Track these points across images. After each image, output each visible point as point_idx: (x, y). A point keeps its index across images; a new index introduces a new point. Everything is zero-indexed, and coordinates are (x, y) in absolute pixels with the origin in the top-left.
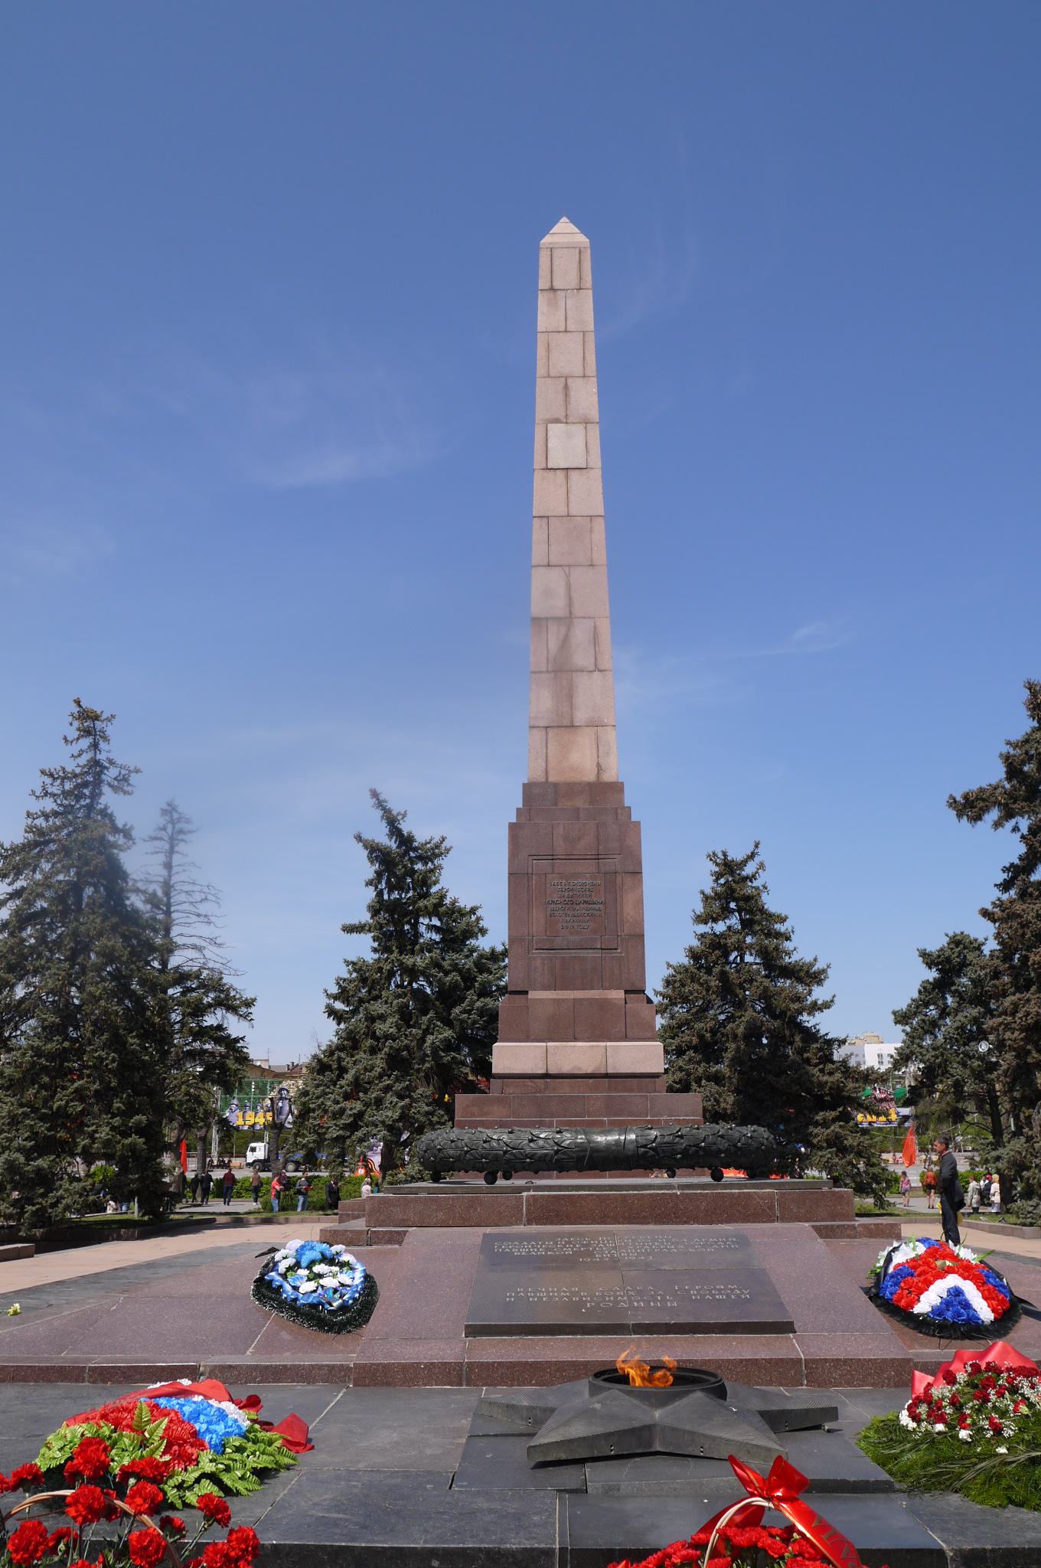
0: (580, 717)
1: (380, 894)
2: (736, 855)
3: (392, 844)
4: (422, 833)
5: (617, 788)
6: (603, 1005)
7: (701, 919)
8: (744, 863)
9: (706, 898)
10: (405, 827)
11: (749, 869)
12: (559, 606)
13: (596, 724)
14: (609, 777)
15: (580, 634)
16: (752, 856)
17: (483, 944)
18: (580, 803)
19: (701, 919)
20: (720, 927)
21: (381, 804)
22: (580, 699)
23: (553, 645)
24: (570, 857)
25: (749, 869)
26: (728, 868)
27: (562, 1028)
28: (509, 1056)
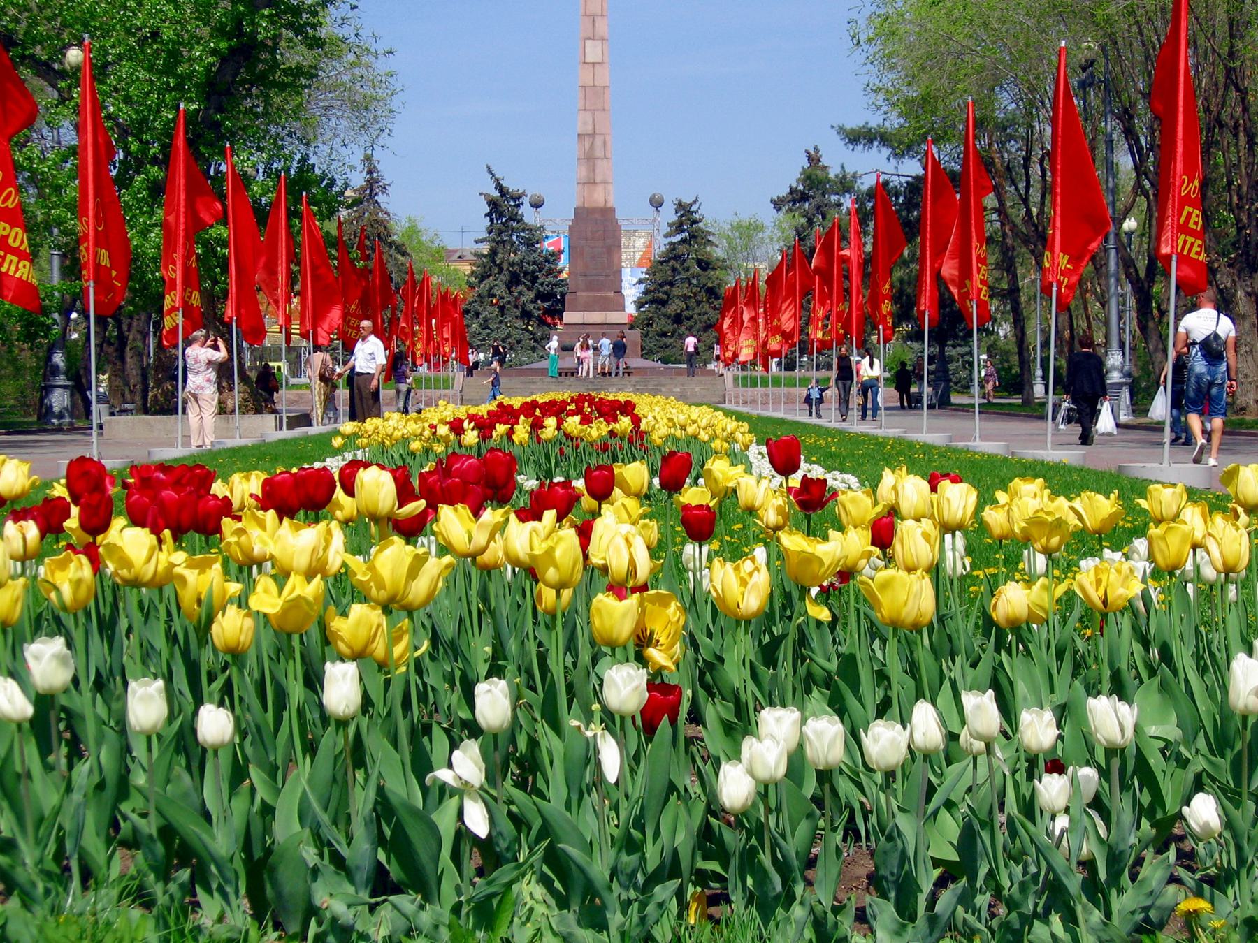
0: (598, 179)
1: (492, 220)
2: (687, 200)
3: (496, 194)
4: (511, 185)
5: (612, 210)
6: (606, 298)
7: (666, 236)
8: (691, 205)
9: (670, 225)
10: (504, 184)
11: (694, 208)
12: (589, 129)
13: (605, 182)
14: (609, 205)
15: (599, 142)
16: (695, 202)
17: (547, 246)
18: (598, 216)
19: (666, 236)
20: (678, 238)
21: (490, 172)
22: (597, 171)
23: (587, 147)
24: (593, 239)
25: (694, 208)
26: (680, 206)
27: (588, 307)
28: (569, 317)
